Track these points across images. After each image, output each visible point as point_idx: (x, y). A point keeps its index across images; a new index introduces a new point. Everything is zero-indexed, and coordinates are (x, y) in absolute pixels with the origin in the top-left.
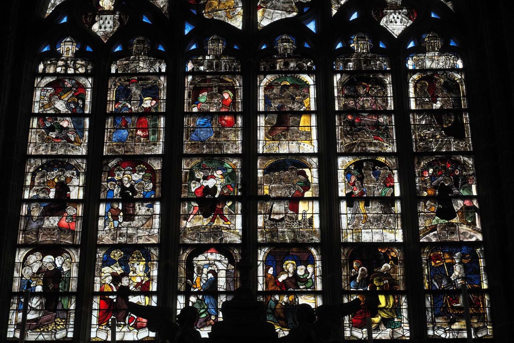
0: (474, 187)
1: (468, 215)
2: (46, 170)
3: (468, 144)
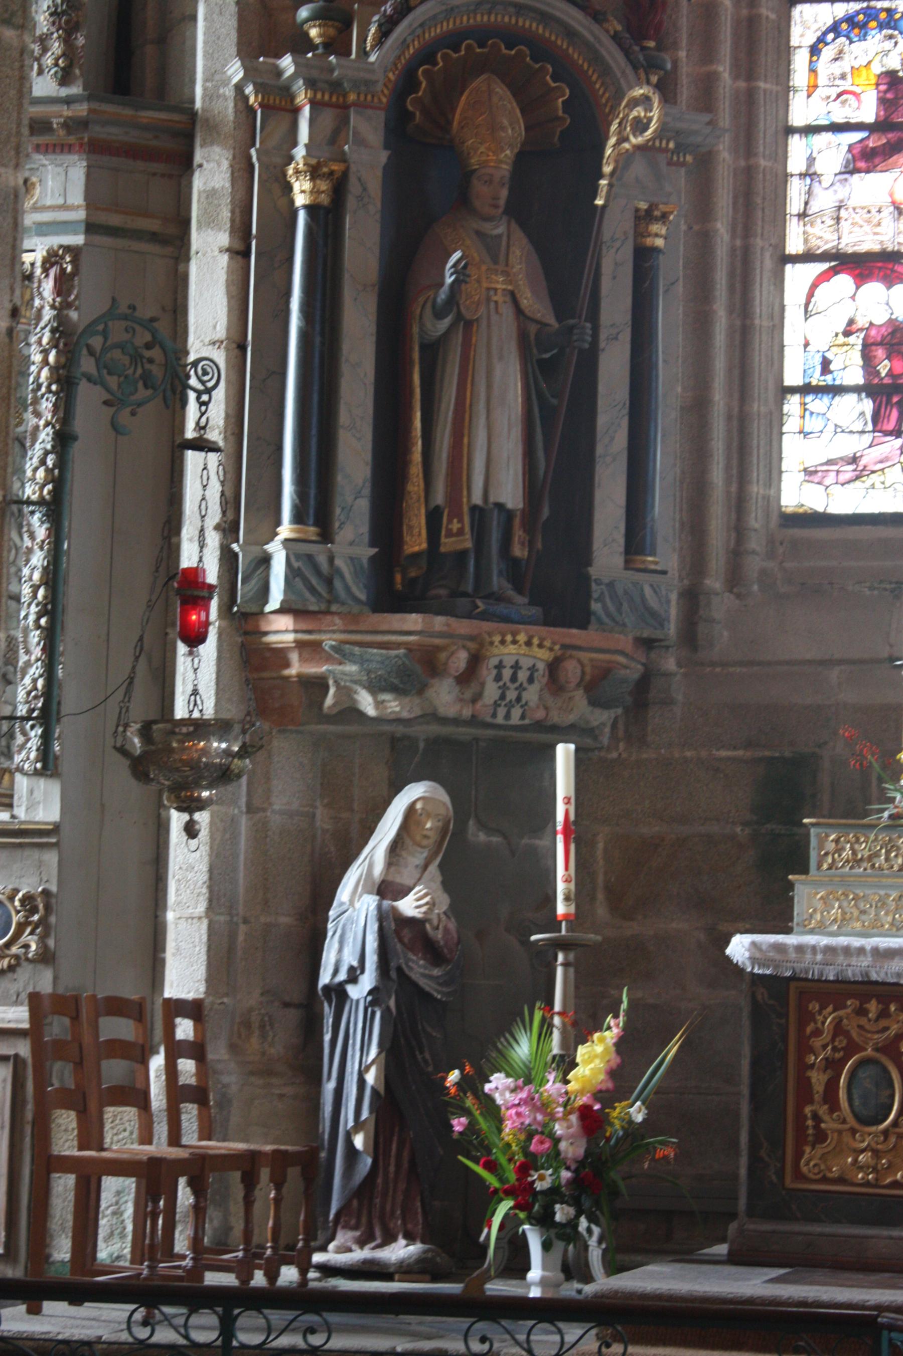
2: (848, 38)
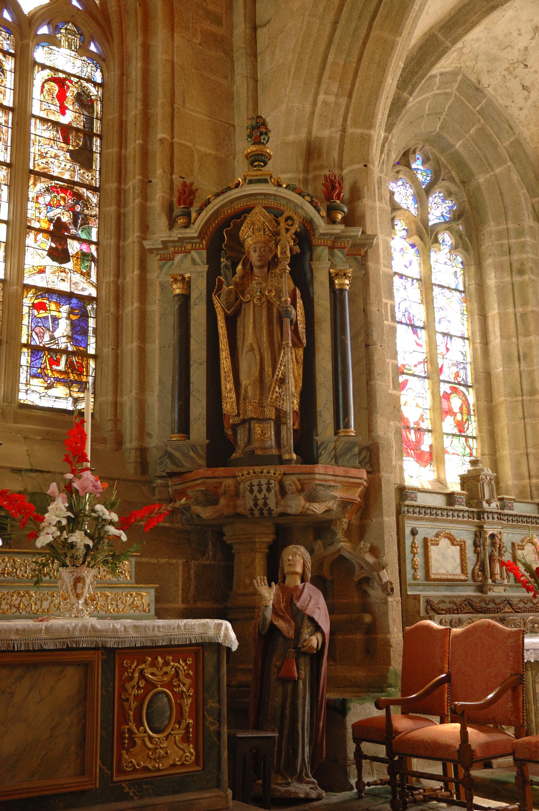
0: (94, 231)
1: (83, 262)
3: (93, 177)
